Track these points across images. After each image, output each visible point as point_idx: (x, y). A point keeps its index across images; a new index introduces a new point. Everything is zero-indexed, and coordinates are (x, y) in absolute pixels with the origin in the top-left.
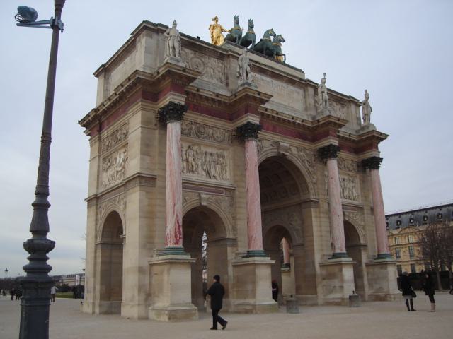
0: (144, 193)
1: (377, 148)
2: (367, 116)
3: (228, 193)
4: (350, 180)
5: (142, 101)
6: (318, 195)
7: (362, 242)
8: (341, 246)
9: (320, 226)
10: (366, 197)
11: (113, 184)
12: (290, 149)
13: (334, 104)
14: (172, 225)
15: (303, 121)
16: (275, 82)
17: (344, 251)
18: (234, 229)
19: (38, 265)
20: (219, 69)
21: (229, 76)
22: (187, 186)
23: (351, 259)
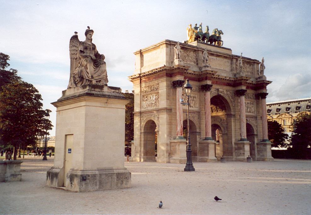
0: (168, 115)
1: (266, 88)
2: (262, 71)
3: (197, 113)
4: (251, 103)
5: (166, 78)
6: (235, 112)
7: (255, 133)
8: (244, 135)
9: (235, 126)
10: (258, 112)
11: (150, 108)
12: (223, 91)
13: (246, 65)
14: (179, 128)
15: (230, 78)
16: (218, 58)
17: (246, 138)
18: (200, 128)
19: (190, 148)
20: (194, 57)
21: (198, 60)
22: (184, 111)
23: (249, 142)
